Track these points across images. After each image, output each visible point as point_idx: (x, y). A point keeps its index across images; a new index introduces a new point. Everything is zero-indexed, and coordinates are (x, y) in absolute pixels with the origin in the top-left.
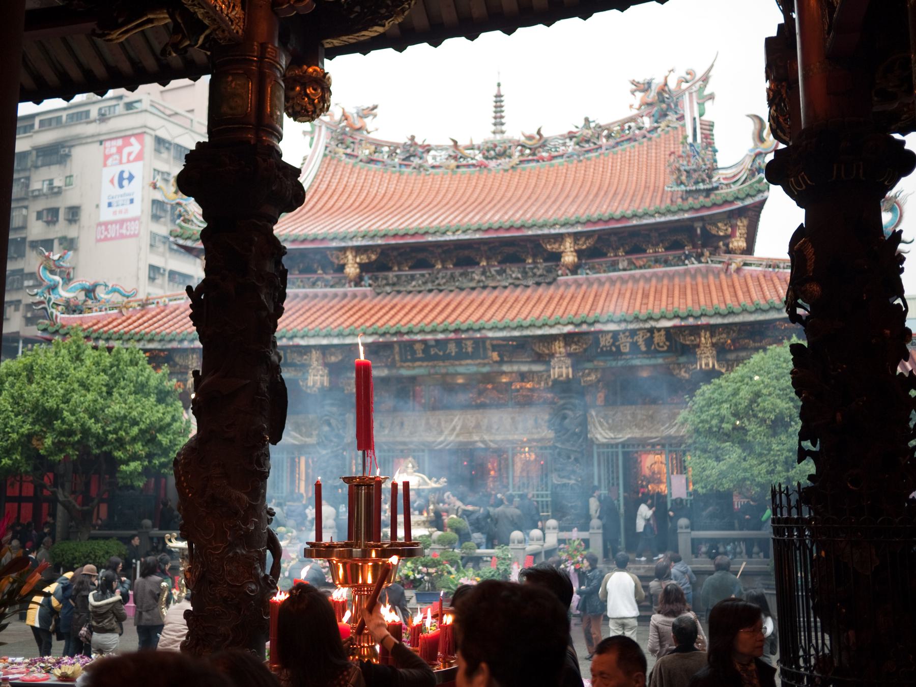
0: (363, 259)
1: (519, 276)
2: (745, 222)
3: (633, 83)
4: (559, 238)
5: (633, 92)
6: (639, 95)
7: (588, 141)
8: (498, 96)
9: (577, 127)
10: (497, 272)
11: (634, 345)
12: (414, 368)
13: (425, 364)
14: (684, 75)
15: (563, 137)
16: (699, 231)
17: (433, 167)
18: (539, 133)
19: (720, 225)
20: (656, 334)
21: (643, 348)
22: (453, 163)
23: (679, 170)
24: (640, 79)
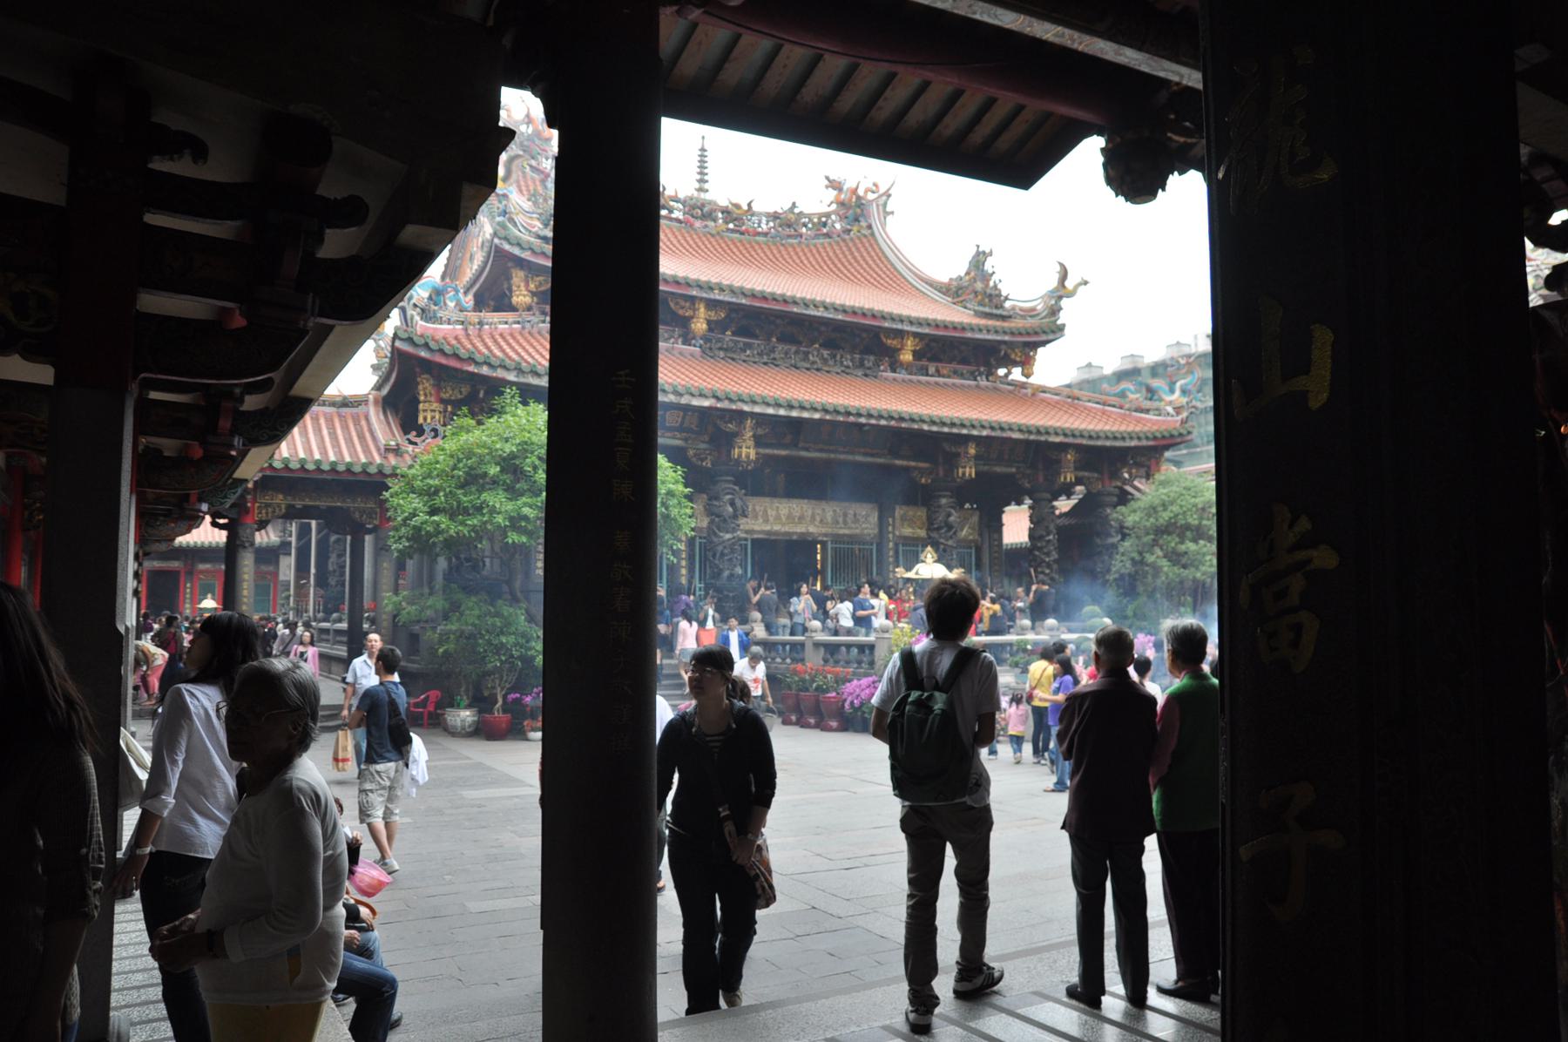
0: (713, 315)
4: (900, 334)
7: (789, 226)
8: (703, 150)
15: (768, 215)
18: (749, 205)
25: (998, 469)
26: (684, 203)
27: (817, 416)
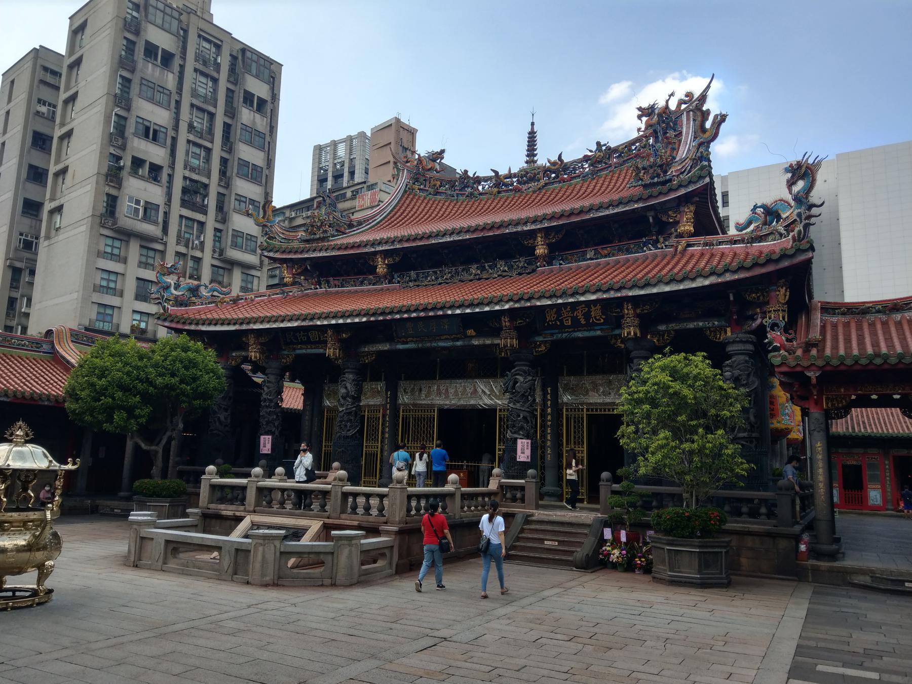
1: (506, 268)
2: (692, 208)
3: (640, 109)
4: (532, 234)
5: (639, 117)
6: (644, 119)
7: (600, 162)
9: (591, 151)
10: (490, 266)
11: (575, 320)
12: (407, 343)
13: (415, 339)
14: (683, 97)
16: (651, 220)
17: (481, 194)
19: (670, 213)
20: (593, 308)
21: (583, 322)
22: (496, 190)
23: (637, 167)
24: (645, 105)
25: (580, 334)
26: (515, 175)
27: (364, 319)
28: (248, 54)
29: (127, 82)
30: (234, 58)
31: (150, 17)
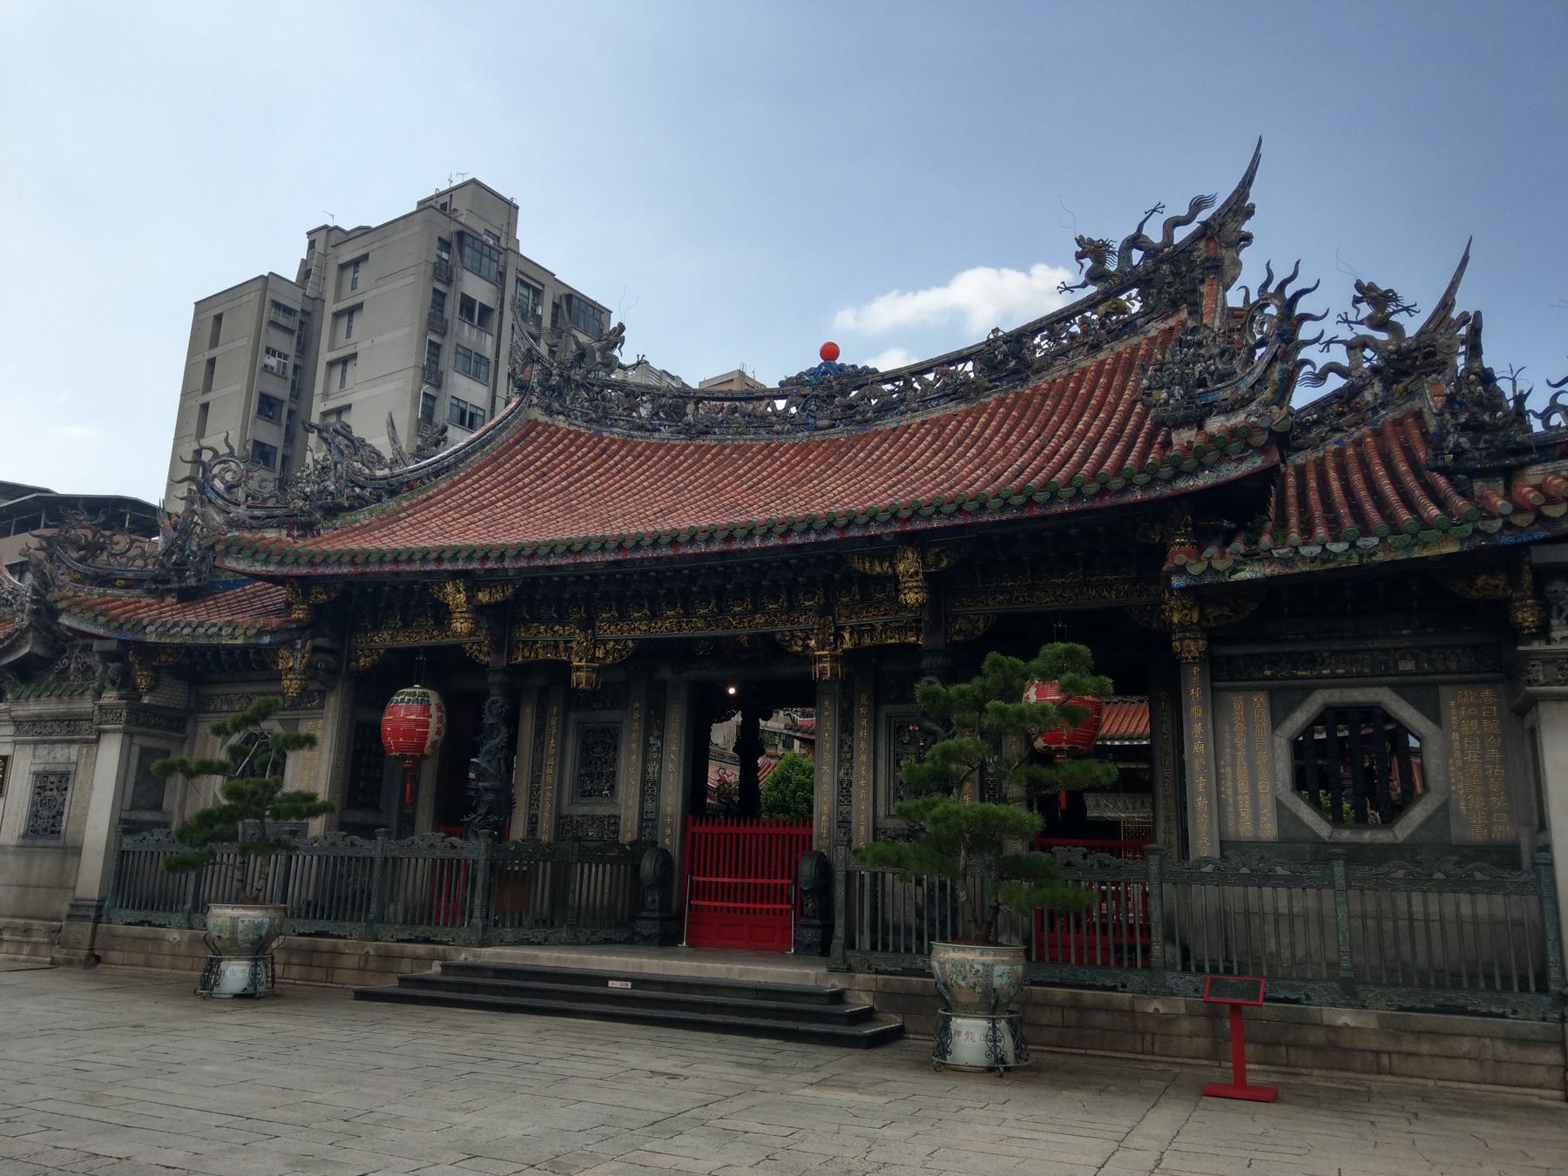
28: (575, 302)
29: (435, 348)
30: (556, 306)
31: (468, 262)
